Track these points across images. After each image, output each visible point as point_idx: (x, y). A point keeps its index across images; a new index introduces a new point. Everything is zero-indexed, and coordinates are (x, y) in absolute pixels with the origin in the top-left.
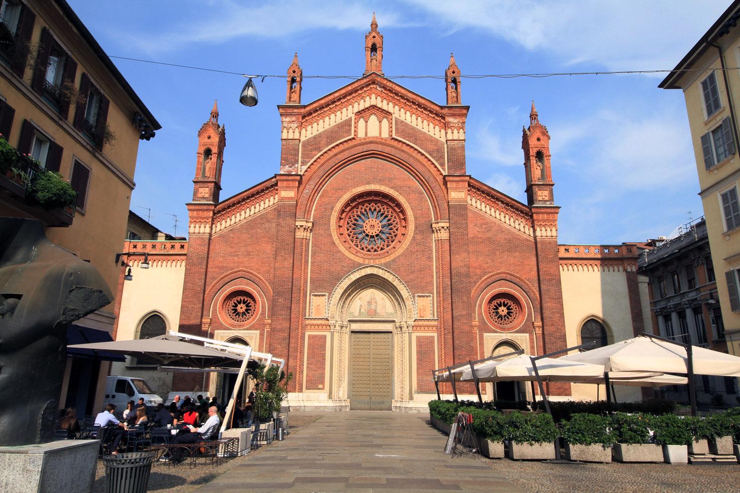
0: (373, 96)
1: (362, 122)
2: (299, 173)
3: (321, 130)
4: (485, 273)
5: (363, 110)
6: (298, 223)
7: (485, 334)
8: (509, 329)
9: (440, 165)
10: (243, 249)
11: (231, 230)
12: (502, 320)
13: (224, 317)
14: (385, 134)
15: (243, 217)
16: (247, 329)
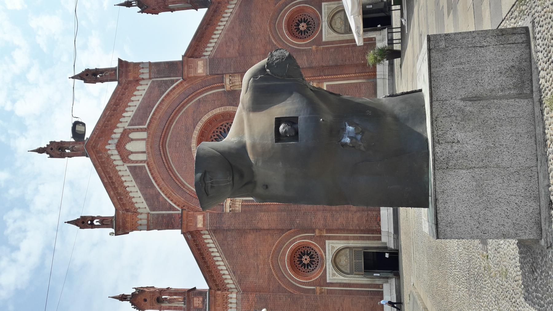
0: (107, 147)
1: (132, 157)
2: (180, 212)
3: (139, 194)
4: (270, 42)
5: (121, 156)
6: (228, 210)
7: (324, 40)
8: (319, 20)
9: (173, 84)
10: (252, 261)
11: (234, 273)
12: (311, 27)
13: (316, 276)
14: (144, 135)
15: (222, 263)
16: (325, 252)
